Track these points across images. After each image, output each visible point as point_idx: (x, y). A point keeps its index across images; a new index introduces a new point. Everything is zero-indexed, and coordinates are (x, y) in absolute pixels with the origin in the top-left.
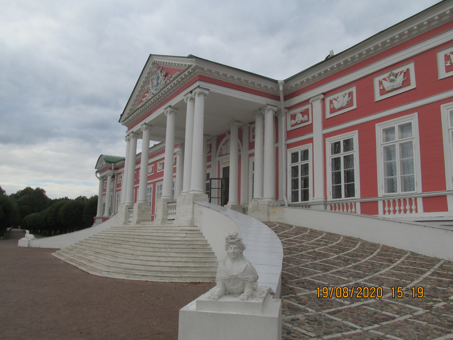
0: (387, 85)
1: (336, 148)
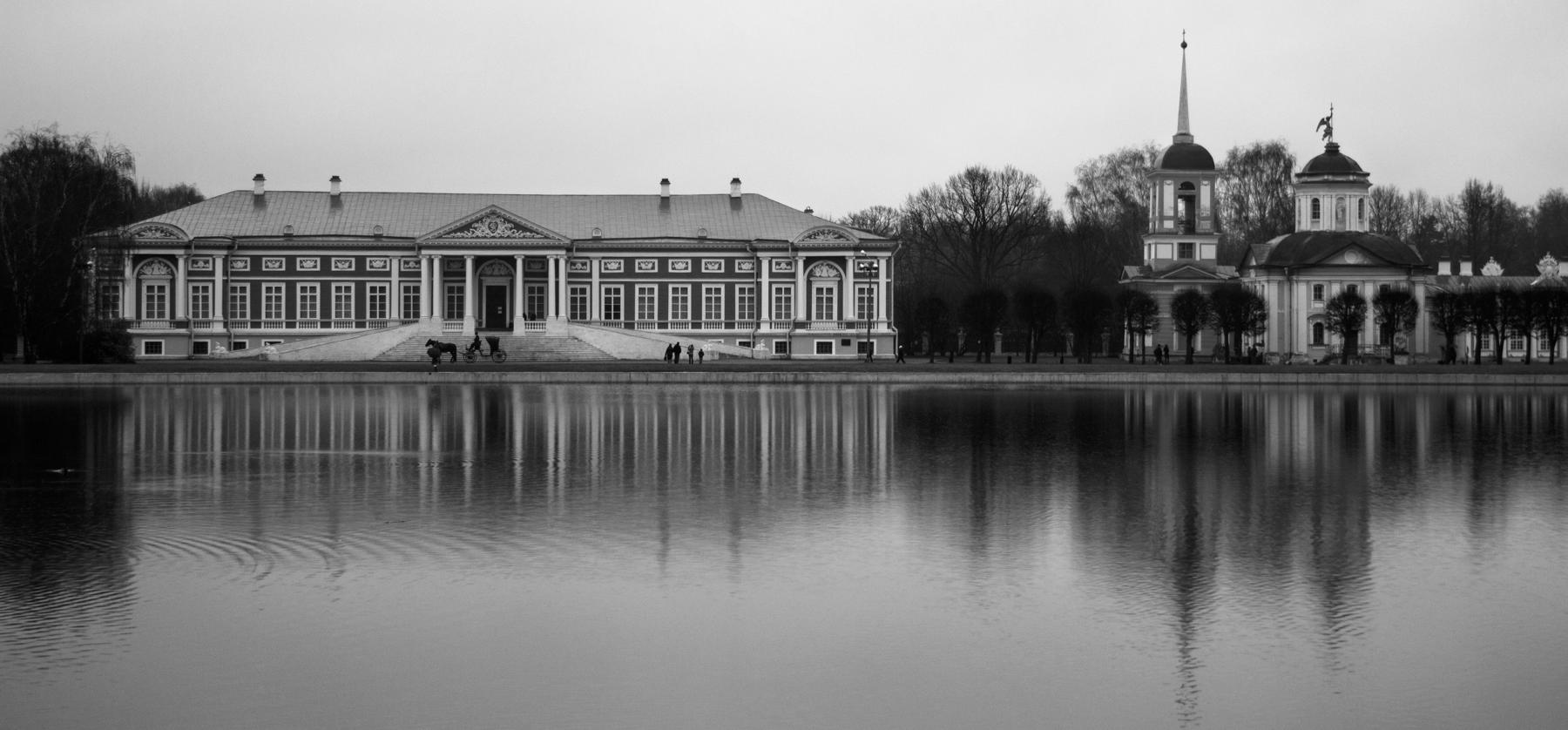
1: (608, 291)
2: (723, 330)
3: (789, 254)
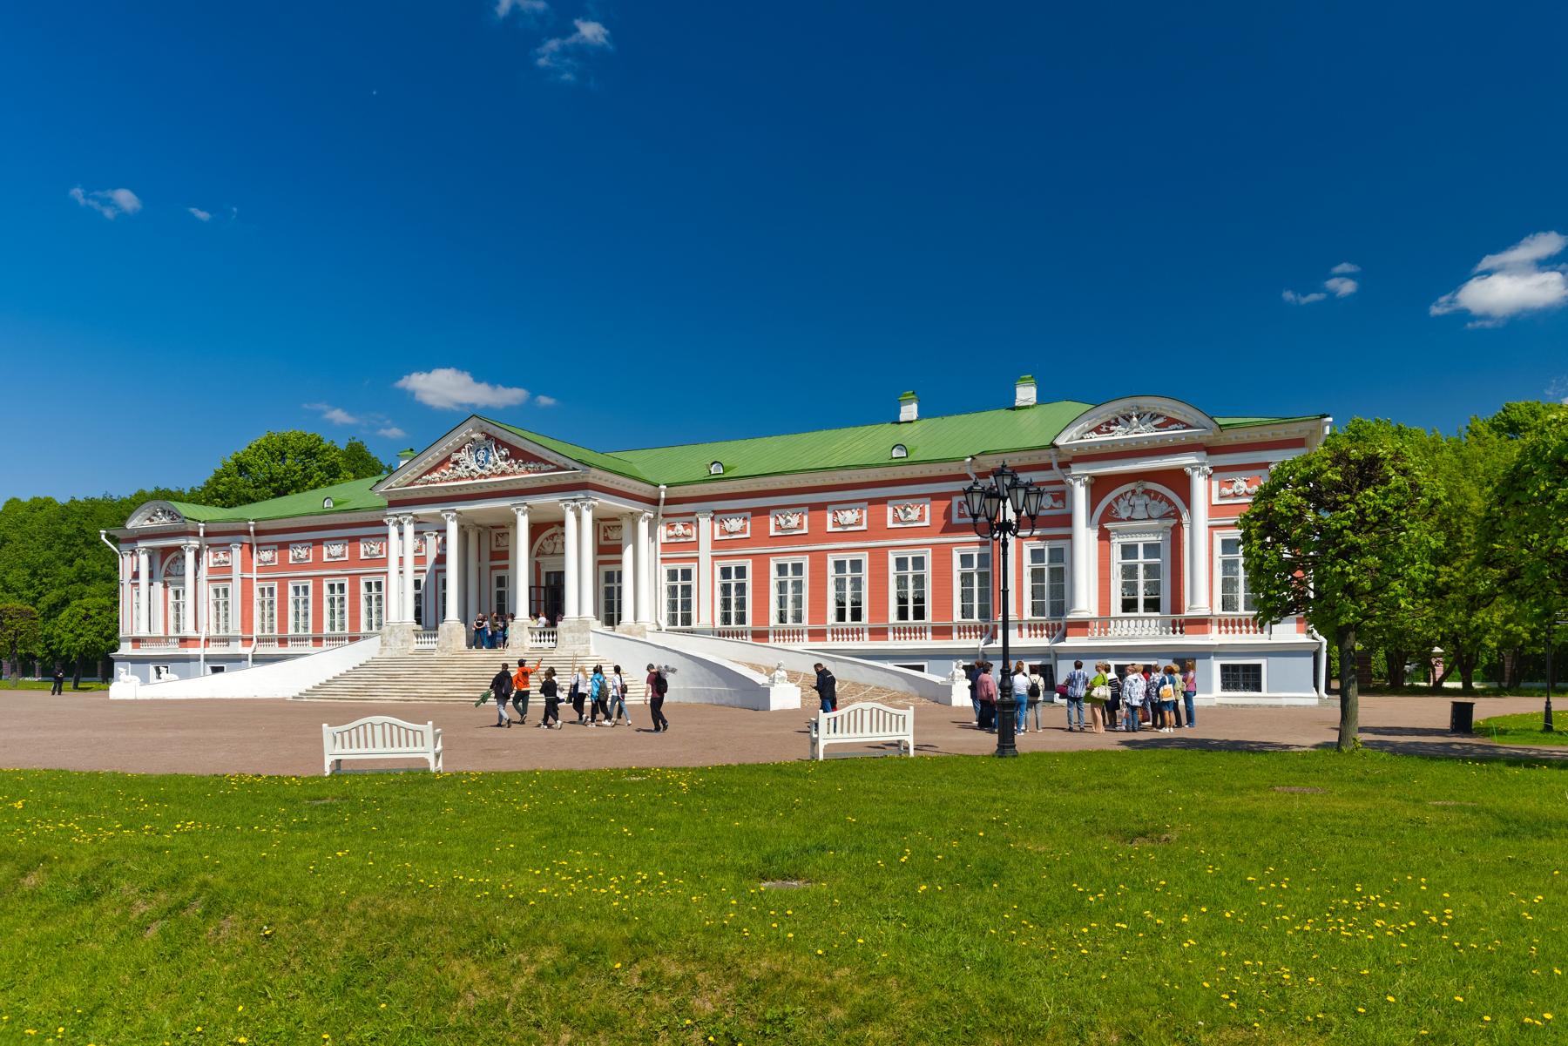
1: (726, 573)
2: (929, 643)
3: (1055, 474)
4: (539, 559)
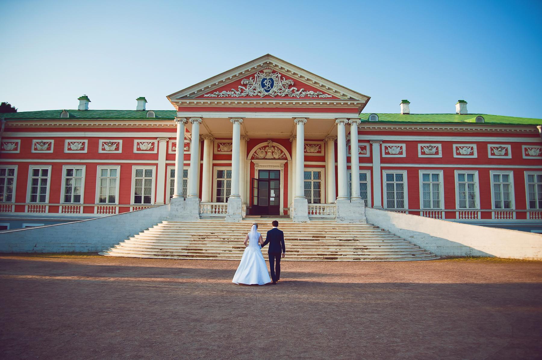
0: (426, 150)
1: (390, 177)
4: (253, 161)
